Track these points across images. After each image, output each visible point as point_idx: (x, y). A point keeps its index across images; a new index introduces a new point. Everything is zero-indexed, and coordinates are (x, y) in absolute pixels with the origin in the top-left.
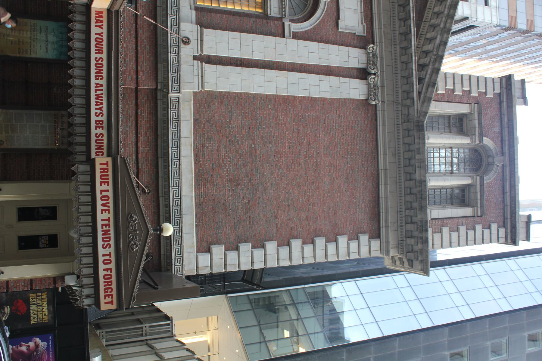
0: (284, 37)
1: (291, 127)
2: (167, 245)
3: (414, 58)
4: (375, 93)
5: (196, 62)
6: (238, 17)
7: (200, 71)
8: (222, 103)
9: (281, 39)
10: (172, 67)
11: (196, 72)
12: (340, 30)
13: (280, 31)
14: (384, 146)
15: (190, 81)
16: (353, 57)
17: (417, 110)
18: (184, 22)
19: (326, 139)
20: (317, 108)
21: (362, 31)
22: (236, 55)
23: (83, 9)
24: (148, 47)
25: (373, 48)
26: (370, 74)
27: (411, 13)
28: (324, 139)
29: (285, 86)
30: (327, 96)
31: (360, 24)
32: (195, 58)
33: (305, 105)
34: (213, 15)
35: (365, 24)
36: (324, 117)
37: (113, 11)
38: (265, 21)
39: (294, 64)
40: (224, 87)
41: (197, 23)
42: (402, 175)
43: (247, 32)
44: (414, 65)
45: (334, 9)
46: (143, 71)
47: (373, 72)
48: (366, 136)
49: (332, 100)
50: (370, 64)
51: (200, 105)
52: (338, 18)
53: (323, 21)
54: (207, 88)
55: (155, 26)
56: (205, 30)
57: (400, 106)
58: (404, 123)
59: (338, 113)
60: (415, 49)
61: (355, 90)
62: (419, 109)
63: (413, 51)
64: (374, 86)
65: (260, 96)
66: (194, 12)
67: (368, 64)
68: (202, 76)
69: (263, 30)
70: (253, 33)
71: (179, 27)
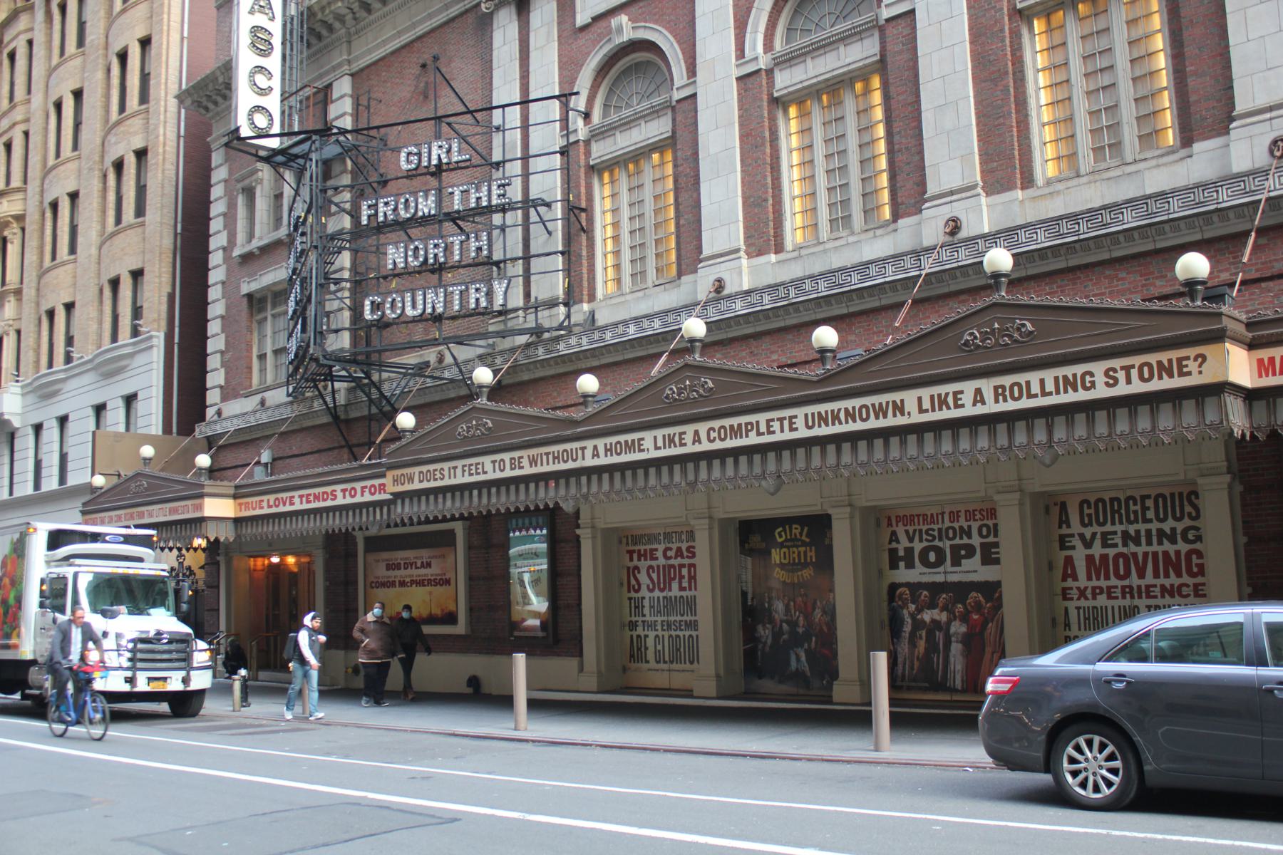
6: (1186, 33)
18: (1230, 165)
23: (1260, 406)
34: (1193, 98)
37: (1250, 335)
41: (1226, 131)
55: (1261, 232)
56: (1241, 106)
66: (1198, 147)
71: (1248, 174)
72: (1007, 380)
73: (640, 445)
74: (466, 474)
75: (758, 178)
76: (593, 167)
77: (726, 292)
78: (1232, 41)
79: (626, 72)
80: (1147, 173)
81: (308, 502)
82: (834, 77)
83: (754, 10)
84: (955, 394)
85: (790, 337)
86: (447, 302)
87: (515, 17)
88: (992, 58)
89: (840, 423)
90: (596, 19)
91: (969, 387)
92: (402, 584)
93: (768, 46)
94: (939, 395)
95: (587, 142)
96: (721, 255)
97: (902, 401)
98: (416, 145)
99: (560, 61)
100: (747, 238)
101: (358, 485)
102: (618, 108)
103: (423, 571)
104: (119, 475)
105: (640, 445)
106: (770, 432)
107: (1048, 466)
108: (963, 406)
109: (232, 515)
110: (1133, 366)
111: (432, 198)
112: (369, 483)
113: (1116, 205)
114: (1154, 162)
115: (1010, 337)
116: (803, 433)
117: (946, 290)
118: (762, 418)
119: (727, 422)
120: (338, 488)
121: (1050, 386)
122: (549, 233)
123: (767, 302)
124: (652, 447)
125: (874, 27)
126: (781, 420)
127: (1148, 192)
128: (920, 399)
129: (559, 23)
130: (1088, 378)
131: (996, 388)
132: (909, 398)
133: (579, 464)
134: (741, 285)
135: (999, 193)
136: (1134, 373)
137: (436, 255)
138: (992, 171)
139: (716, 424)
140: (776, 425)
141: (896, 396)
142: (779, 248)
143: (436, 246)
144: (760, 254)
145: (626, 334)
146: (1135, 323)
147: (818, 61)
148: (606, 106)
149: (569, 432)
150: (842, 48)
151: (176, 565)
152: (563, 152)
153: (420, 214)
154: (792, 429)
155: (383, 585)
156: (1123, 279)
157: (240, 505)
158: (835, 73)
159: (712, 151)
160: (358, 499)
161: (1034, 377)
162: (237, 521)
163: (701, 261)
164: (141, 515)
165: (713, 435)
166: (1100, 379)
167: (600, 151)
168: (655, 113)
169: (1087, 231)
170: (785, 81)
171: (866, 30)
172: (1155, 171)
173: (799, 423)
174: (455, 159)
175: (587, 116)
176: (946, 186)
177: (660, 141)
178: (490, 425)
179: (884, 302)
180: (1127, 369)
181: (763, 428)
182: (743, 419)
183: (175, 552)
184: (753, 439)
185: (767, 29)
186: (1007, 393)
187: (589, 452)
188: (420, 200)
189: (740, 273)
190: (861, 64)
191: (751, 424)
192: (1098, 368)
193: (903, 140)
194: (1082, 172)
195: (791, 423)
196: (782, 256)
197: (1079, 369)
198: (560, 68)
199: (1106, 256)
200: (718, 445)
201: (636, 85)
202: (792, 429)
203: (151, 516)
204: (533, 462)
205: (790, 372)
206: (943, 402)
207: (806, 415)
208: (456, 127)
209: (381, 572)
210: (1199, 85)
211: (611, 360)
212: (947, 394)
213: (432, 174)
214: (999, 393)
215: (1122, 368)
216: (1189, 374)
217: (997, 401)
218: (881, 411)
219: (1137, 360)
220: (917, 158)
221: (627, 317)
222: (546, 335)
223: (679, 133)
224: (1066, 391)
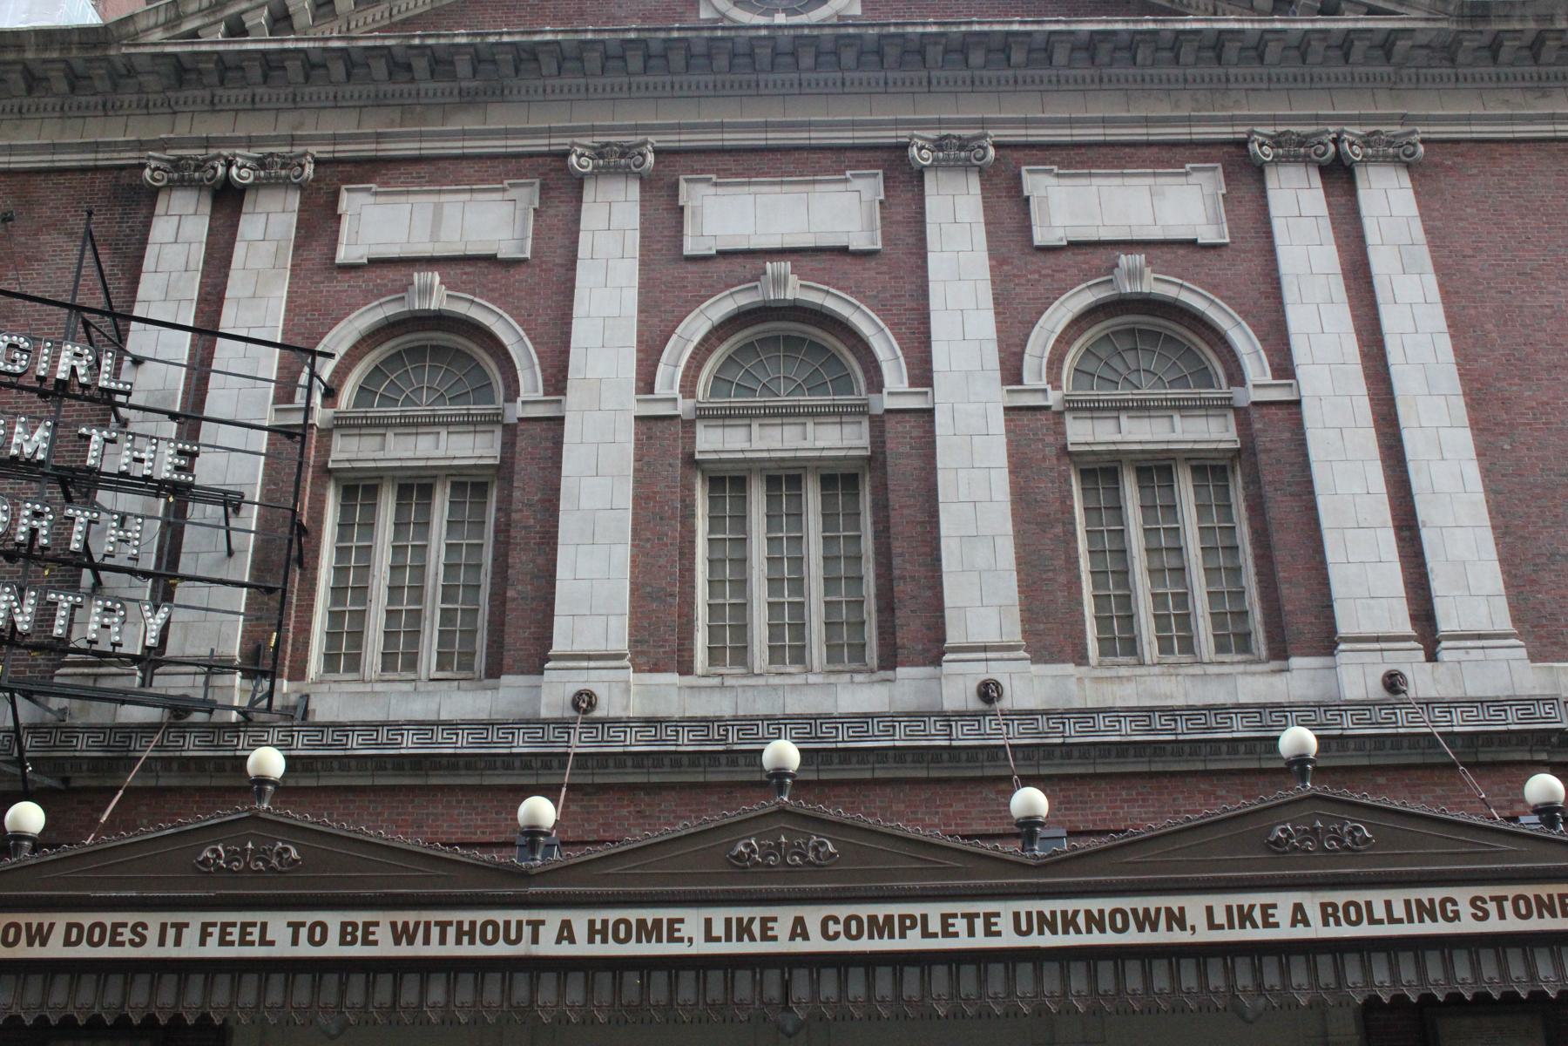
0: (1298, 403)
1: (1548, 388)
2: (1180, 753)
3: (1278, 26)
4: (1389, 144)
5: (1444, 655)
7: (1469, 643)
8: (1533, 582)
9: (1309, 412)
10: (1489, 722)
11: (1475, 654)
12: (1227, 240)
13: (1282, 413)
14: (1531, 120)
15: (1488, 671)
16: (1296, 200)
17: (1427, 20)
19: (1553, 288)
20: (1473, 312)
21: (1210, 174)
22: (1387, 539)
24: (1439, 791)
25: (1261, 145)
26: (1338, 155)
27: (1145, 26)
28: (1554, 293)
29: (1441, 401)
30: (1431, 280)
31: (1191, 179)
32: (1432, 657)
33: (1474, 345)
35: (1188, 166)
36: (1493, 292)
38: (1262, 457)
39: (1367, 377)
40: (1488, 575)
42: (823, 75)
43: (1312, 508)
44: (1299, 26)
45: (1169, 257)
46: (1512, 802)
47: (1332, 148)
48: (1510, 173)
49: (1439, 268)
50: (1307, 156)
51: (1555, 644)
52: (1192, 243)
53: (1214, 288)
54: (1504, 623)
57: (1405, 72)
58: (1453, 60)
59: (1470, 252)
60: (1252, 21)
61: (1388, 200)
62: (1425, 15)
63: (1257, 26)
64: (1367, 144)
65: (1487, 473)
66: (1295, 662)
67: (1306, 160)
68: (1480, 637)
69: (1292, 465)
70: (1311, 492)
72: (1340, 897)
73: (671, 930)
74: (213, 941)
75: (662, 561)
76: (330, 471)
77: (597, 714)
78: (1330, 556)
79: (416, 353)
80: (1241, 680)
82: (795, 459)
83: (674, 337)
84: (1264, 908)
85: (714, 798)
86: (46, 613)
87: (206, 208)
88: (1039, 498)
89: (1078, 931)
90: (375, 263)
91: (1284, 902)
93: (688, 388)
94: (740, 920)
95: (326, 433)
96: (589, 658)
97: (1182, 910)
98: (30, 338)
99: (290, 301)
100: (635, 642)
102: (386, 400)
105: (671, 930)
106: (946, 934)
107: (332, 1038)
108: (1276, 925)
110: (1505, 898)
111: (41, 433)
113: (1223, 707)
114: (1241, 668)
115: (1340, 841)
116: (1008, 939)
117: (978, 773)
118: (934, 911)
119: (864, 911)
121: (1399, 911)
122: (230, 553)
123: (686, 743)
124: (699, 936)
125: (863, 413)
126: (970, 918)
127: (1242, 700)
128: (1210, 910)
129: (297, 248)
130: (1449, 906)
131: (1324, 906)
132: (1194, 906)
133: (523, 949)
134: (627, 708)
135: (1046, 662)
136: (1508, 906)
137: (34, 532)
138: (1037, 634)
139: (842, 911)
140: (960, 925)
141: (1174, 902)
142: (686, 668)
143: (37, 515)
144: (655, 668)
145: (392, 743)
146: (1526, 847)
147: (769, 431)
148: (364, 392)
149: (510, 891)
150: (810, 427)
152: (279, 432)
153: (14, 451)
154: (989, 933)
156: (1222, 797)
158: (799, 454)
159: (585, 504)
161: (1377, 898)
163: (548, 660)
165: (832, 928)
166: (1466, 910)
167: (346, 451)
168: (471, 424)
169: (1186, 732)
170: (711, 441)
171: (850, 414)
172: (1249, 679)
173: (1005, 926)
174: (103, 383)
175: (330, 394)
176: (976, 638)
177: (475, 466)
178: (294, 854)
179: (879, 774)
180: (1500, 900)
181: (935, 926)
182: (896, 910)
184: (914, 941)
185: (688, 367)
186: (1341, 914)
187: (548, 933)
188: (18, 429)
189: (628, 690)
190: (842, 453)
191: (912, 917)
192: (1463, 895)
193: (908, 566)
194: (1147, 659)
195: (988, 925)
196: (688, 680)
197: (1438, 894)
198: (288, 310)
199: (1200, 766)
200: (843, 945)
201: (429, 377)
202: (989, 933)
204: (402, 934)
205: (987, 847)
206: (1246, 917)
207: (1017, 916)
208: (94, 334)
210: (1293, 595)
211: (345, 782)
212: (751, 920)
213: (43, 394)
214: (1329, 913)
215: (1492, 899)
216: (956, 935)
217: (1326, 923)
218: (1147, 921)
219: (1510, 891)
220: (929, 593)
221: (381, 717)
222: (198, 717)
223: (520, 464)
224: (1421, 920)
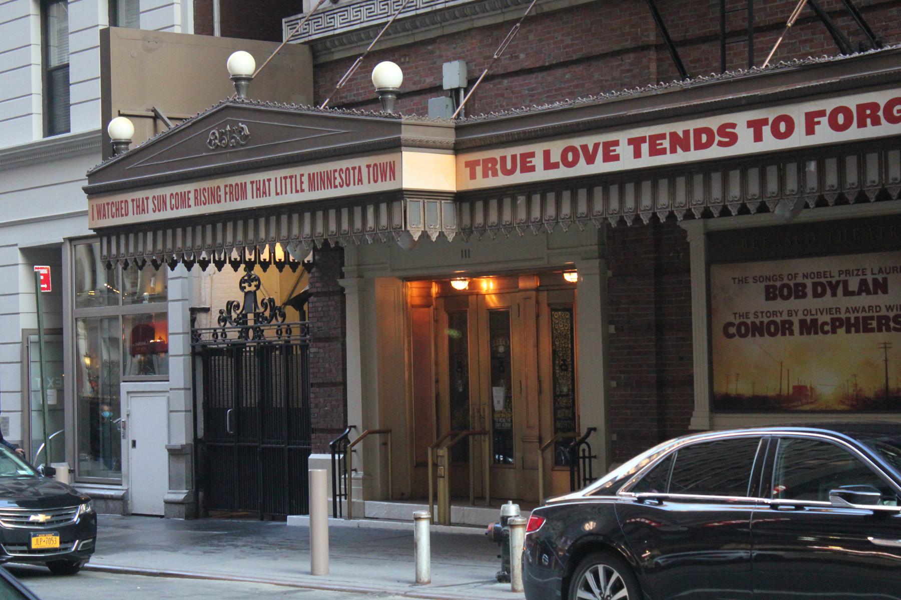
81: (654, 152)
92: (810, 327)
101: (798, 112)
103: (864, 300)
104: (156, 117)
109: (450, 186)
112: (829, 105)
120: (740, 119)
151: (239, 297)
155: (758, 330)
157: (471, 165)
160: (798, 139)
162: (460, 198)
164: (240, 192)
183: (242, 272)
203: (261, 191)
209: (754, 302)
